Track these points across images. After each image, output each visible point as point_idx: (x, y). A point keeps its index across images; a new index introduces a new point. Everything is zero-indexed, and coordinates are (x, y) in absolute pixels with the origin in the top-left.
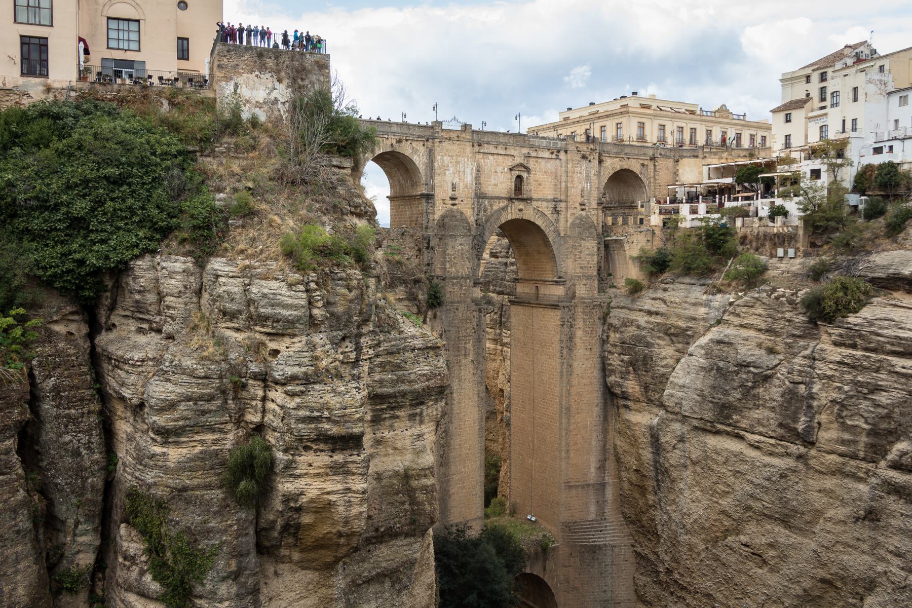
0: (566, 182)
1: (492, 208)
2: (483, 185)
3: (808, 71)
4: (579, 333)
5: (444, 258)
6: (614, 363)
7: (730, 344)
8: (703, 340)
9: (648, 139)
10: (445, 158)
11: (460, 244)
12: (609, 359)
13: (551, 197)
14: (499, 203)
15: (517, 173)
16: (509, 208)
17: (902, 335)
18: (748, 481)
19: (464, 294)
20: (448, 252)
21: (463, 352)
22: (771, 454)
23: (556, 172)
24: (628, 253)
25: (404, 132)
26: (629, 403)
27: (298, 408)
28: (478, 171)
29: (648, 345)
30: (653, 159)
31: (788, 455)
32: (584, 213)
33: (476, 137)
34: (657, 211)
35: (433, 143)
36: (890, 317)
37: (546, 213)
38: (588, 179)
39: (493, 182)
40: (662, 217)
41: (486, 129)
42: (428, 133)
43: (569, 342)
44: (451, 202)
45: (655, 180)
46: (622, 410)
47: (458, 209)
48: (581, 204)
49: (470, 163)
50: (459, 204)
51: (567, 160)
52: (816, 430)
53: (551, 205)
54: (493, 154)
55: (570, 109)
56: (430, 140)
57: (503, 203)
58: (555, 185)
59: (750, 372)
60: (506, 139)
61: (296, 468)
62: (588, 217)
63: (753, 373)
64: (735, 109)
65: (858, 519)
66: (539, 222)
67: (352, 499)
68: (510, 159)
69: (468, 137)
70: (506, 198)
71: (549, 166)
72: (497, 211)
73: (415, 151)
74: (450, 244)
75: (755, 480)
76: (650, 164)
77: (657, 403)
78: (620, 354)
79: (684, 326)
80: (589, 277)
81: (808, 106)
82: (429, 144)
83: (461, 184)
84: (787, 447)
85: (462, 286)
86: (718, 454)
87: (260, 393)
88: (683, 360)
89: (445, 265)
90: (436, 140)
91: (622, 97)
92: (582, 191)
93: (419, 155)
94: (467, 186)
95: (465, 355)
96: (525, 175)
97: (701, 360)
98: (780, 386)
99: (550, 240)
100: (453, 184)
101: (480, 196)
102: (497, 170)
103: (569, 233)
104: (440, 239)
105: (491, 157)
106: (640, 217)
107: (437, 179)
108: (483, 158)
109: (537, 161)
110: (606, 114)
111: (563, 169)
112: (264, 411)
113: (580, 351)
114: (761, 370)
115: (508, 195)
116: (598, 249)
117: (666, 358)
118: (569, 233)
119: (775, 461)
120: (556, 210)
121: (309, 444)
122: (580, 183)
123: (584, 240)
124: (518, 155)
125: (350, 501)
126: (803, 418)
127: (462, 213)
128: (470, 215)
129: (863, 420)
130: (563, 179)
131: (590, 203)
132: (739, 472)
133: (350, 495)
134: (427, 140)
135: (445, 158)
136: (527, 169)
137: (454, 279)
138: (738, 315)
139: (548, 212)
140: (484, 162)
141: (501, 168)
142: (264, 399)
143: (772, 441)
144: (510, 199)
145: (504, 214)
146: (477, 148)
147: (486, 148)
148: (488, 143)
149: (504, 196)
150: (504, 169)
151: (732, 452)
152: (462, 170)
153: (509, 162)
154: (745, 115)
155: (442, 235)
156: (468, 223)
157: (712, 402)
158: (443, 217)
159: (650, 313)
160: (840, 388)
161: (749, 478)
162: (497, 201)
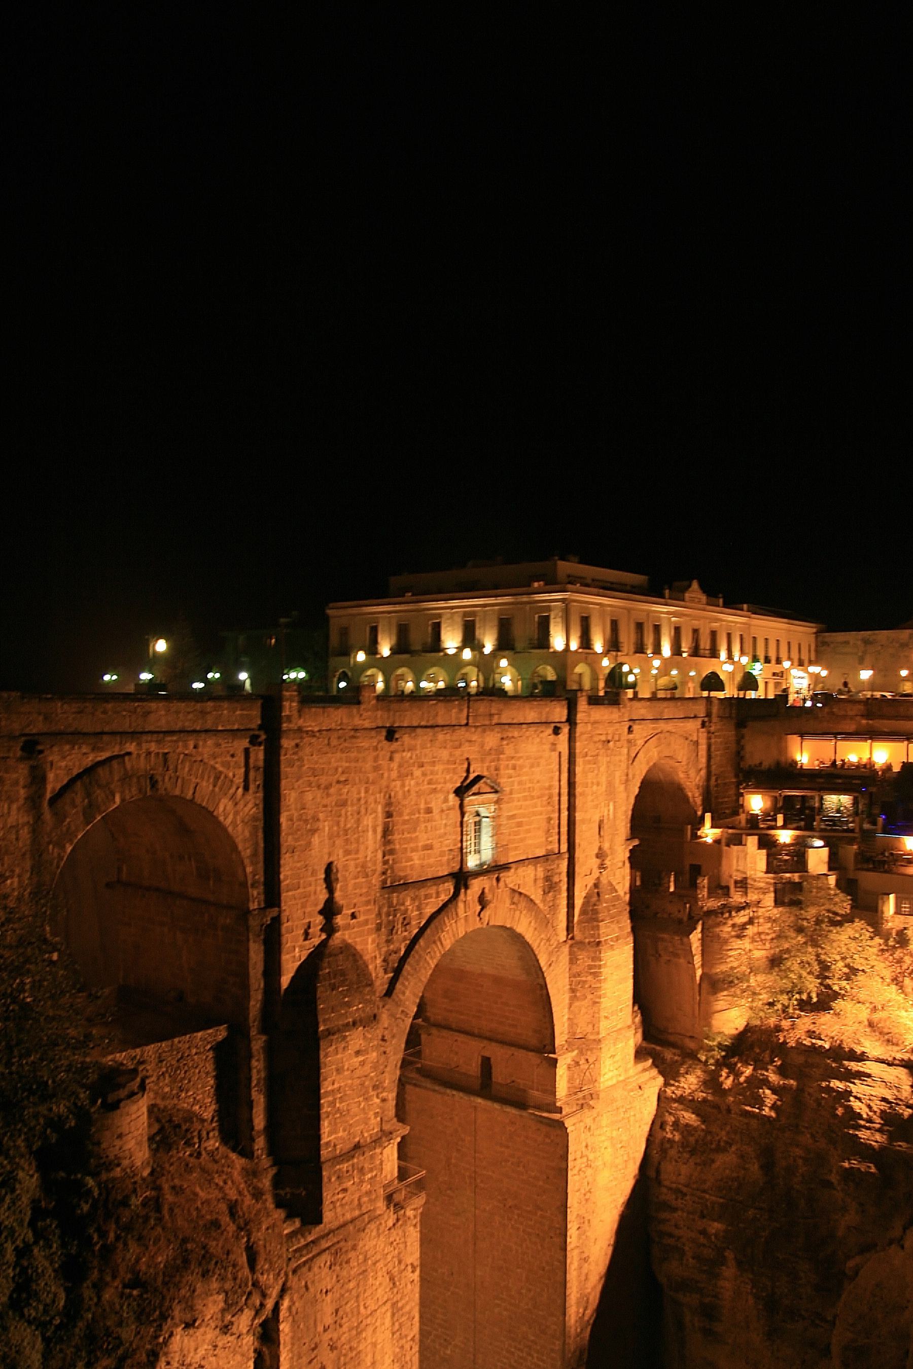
10: (309, 796)
13: (541, 852)
14: (438, 895)
16: (461, 905)
19: (368, 1193)
25: (188, 725)
28: (389, 815)
37: (532, 897)
39: (423, 839)
47: (344, 941)
53: (540, 872)
58: (549, 819)
71: (536, 770)
94: (364, 866)
99: (543, 963)
102: (433, 805)
109: (514, 768)
122: (596, 807)
137: (342, 1162)
140: (403, 786)
141: (441, 797)
162: (432, 890)
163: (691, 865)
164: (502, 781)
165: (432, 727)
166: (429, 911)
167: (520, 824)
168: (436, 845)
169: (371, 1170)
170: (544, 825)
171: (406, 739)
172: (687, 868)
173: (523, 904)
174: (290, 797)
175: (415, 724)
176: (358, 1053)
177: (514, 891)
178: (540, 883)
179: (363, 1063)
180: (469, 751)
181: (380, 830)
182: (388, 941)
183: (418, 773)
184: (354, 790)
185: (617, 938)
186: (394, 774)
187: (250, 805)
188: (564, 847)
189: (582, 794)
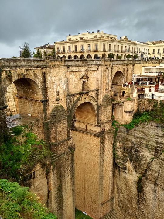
4: (106, 146)
6: (120, 155)
10: (52, 78)
12: (117, 153)
16: (81, 98)
19: (66, 148)
24: (123, 109)
26: (126, 171)
28: (67, 82)
29: (138, 151)
30: (127, 65)
32: (107, 94)
34: (136, 91)
43: (102, 150)
44: (57, 102)
53: (95, 93)
54: (73, 72)
56: (44, 68)
57: (78, 96)
70: (79, 94)
73: (36, 76)
77: (140, 173)
78: (122, 152)
79: (157, 146)
90: (47, 68)
96: (86, 80)
100: (57, 92)
105: (72, 74)
106: (122, 91)
110: (91, 39)
115: (81, 92)
117: (146, 157)
118: (102, 104)
120: (97, 95)
123: (108, 106)
128: (65, 106)
134: (42, 69)
136: (87, 77)
137: (61, 143)
139: (94, 96)
144: (81, 94)
148: (71, 66)
153: (80, 75)
155: (54, 122)
158: (53, 111)
159: (137, 137)
163: (123, 91)
165: (75, 65)
169: (66, 144)
171: (70, 67)
172: (122, 91)
175: (72, 64)
176: (63, 124)
177: (90, 96)
178: (95, 94)
181: (66, 84)
184: (61, 77)
185: (109, 104)
187: (42, 80)
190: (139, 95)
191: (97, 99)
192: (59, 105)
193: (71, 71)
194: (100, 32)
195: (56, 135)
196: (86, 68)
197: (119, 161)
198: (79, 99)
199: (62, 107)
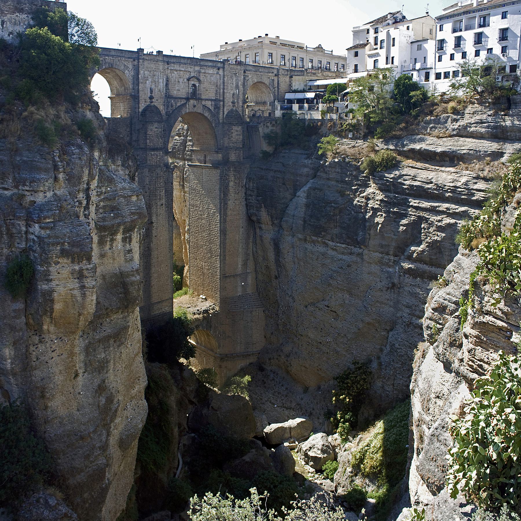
0: (224, 89)
1: (176, 105)
2: (170, 90)
3: (368, 27)
4: (231, 184)
5: (146, 137)
7: (321, 190)
8: (305, 188)
9: (275, 63)
11: (156, 128)
13: (214, 98)
15: (193, 83)
17: (415, 184)
18: (329, 269)
20: (148, 133)
21: (159, 197)
22: (343, 253)
23: (217, 83)
27: (49, 237)
28: (167, 81)
31: (351, 254)
33: (166, 59)
34: (279, 108)
35: (138, 62)
36: (409, 174)
38: (237, 87)
39: (177, 88)
40: (282, 112)
41: (173, 54)
42: (135, 56)
45: (278, 89)
46: (258, 230)
48: (233, 103)
49: (162, 76)
50: (155, 102)
51: (224, 75)
52: (368, 240)
53: (213, 103)
54: (177, 71)
55: (226, 43)
56: (136, 61)
58: (216, 91)
59: (332, 206)
60: (186, 61)
61: (49, 275)
62: (237, 111)
63: (334, 207)
64: (327, 47)
65: (388, 288)
66: (206, 114)
67: (86, 292)
68: (188, 74)
69: (161, 59)
72: (179, 106)
74: (150, 127)
75: (333, 268)
76: (276, 78)
80: (237, 149)
81: (367, 47)
82: (136, 63)
83: (156, 89)
84: (351, 250)
85: (157, 155)
86: (313, 254)
87: (24, 229)
88: (293, 200)
89: (146, 141)
91: (259, 37)
92: (233, 94)
93: (129, 70)
94: (160, 90)
95: (160, 199)
97: (304, 199)
98: (349, 215)
100: (151, 89)
101: (168, 97)
103: (225, 121)
104: (143, 125)
107: (141, 86)
108: (170, 73)
109: (205, 76)
111: (222, 81)
112: (27, 240)
113: (232, 195)
114: (337, 205)
116: (243, 131)
119: (344, 257)
120: (217, 107)
121: (57, 259)
123: (235, 125)
124: (193, 70)
125: (85, 294)
126: (361, 233)
127: (157, 108)
128: (161, 108)
129: (393, 233)
130: (222, 87)
131: (238, 102)
132: (324, 264)
133: (85, 290)
134: (134, 60)
135: (146, 72)
136: (199, 80)
138: (326, 173)
139: (212, 108)
141: (182, 79)
142: (26, 232)
143: (344, 246)
144: (188, 99)
145: (184, 109)
146: (166, 66)
147: (172, 67)
148: (174, 63)
149: (184, 97)
150: (184, 80)
151: (320, 253)
152: (157, 80)
154: (332, 51)
156: (161, 114)
157: (310, 225)
158: (145, 110)
160: (382, 215)
161: (330, 267)
162: (180, 100)
164: (201, 79)
166: (178, 104)
167: (207, 90)
168: (181, 90)
170: (215, 92)
173: (206, 109)
174: (142, 72)
178: (213, 106)
179: (157, 131)
180: (191, 70)
182: (167, 109)
183: (176, 73)
186: (169, 72)
188: (221, 99)
189: (227, 86)
190: (284, 115)
191: (218, 113)
192: (152, 104)
193: (172, 68)
194: (269, 36)
195: (146, 139)
196: (197, 68)
197: (252, 211)
198: (184, 105)
199: (157, 108)
